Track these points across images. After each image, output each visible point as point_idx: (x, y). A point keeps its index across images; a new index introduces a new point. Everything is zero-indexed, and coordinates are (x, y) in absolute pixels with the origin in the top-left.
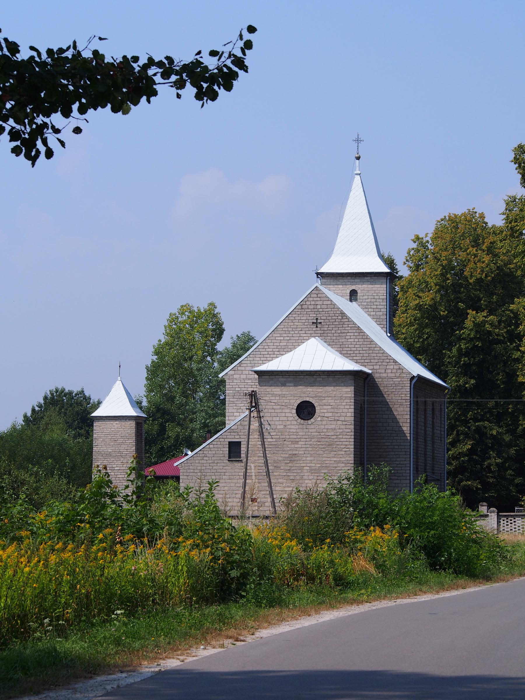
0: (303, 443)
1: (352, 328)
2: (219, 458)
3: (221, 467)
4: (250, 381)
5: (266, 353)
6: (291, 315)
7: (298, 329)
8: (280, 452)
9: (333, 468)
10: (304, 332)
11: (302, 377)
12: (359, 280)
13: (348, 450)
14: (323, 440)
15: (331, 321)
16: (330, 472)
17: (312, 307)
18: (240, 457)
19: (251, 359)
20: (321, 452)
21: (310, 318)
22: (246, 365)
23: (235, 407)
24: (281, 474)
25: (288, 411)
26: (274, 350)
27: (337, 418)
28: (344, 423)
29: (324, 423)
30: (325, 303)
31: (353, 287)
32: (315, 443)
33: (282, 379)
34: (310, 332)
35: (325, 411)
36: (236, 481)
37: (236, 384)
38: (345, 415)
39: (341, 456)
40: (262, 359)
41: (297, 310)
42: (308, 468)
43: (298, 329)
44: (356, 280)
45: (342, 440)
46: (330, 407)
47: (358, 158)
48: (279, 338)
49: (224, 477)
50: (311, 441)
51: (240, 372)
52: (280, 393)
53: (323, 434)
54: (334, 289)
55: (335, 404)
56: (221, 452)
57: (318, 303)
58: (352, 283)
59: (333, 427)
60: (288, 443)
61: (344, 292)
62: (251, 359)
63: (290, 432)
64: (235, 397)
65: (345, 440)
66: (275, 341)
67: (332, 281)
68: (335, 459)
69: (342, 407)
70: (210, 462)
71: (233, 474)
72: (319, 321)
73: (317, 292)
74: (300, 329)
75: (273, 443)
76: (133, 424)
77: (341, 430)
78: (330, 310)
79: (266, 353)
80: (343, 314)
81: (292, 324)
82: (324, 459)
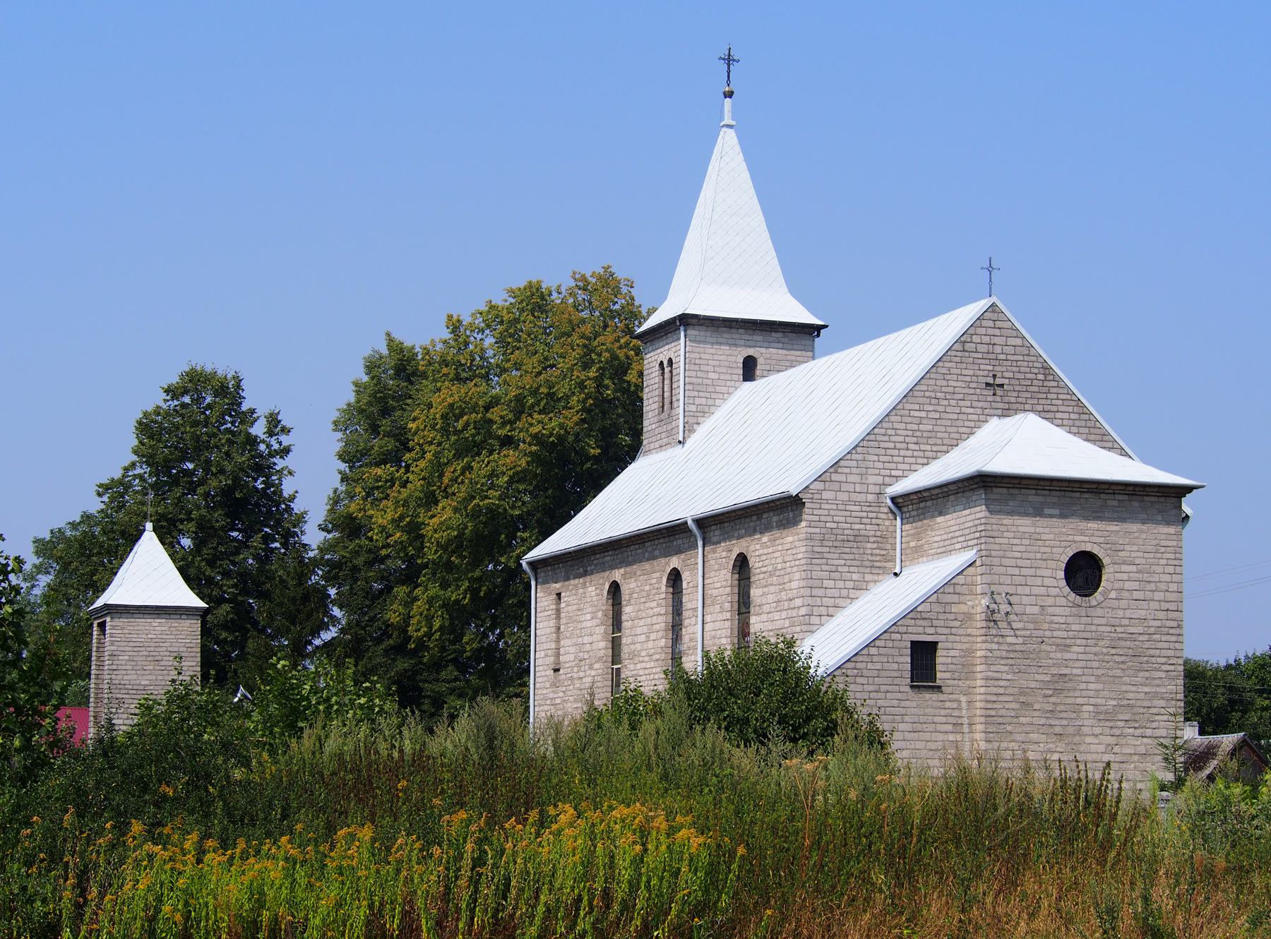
0: (1081, 649)
1: (1066, 403)
2: (889, 681)
3: (895, 703)
4: (858, 508)
5: (892, 445)
6: (940, 364)
7: (957, 396)
8: (1034, 670)
9: (1141, 710)
10: (968, 404)
11: (1078, 495)
12: (760, 338)
13: (1172, 668)
14: (1122, 643)
15: (1023, 382)
16: (1137, 718)
17: (984, 348)
18: (938, 682)
19: (859, 457)
20: (1119, 673)
21: (981, 373)
22: (847, 470)
23: (825, 568)
24: (1036, 721)
25: (1048, 573)
26: (908, 439)
27: (1149, 595)
28: (1165, 605)
29: (1124, 603)
30: (1011, 341)
31: (751, 352)
32: (1105, 650)
33: (1034, 498)
34: (980, 404)
35: (1125, 576)
36: (927, 736)
37: (826, 512)
38: (1165, 588)
39: (1158, 682)
40: (882, 458)
41: (953, 353)
42: (1091, 708)
43: (957, 396)
44: (755, 337)
45: (1160, 645)
46: (1134, 568)
47: (729, 95)
48: (917, 414)
49: (902, 727)
50: (1096, 645)
51: (836, 486)
52: (1032, 530)
53: (1121, 629)
54: (713, 351)
55: (1143, 561)
56: (895, 666)
57: (996, 340)
58: (750, 343)
59: (1142, 613)
60: (1048, 648)
61: (732, 359)
62: (859, 457)
63: (1052, 622)
64: (825, 543)
65: (1166, 645)
66: (909, 420)
67: (708, 334)
68: (1147, 689)
69: (1159, 569)
70: (871, 688)
71: (922, 719)
72: (998, 381)
73: (995, 316)
74: (961, 396)
75: (1018, 648)
76: (196, 625)
77: (1158, 623)
78: (1021, 358)
79: (892, 445)
80: (1046, 369)
81: (944, 383)
82: (1124, 688)
